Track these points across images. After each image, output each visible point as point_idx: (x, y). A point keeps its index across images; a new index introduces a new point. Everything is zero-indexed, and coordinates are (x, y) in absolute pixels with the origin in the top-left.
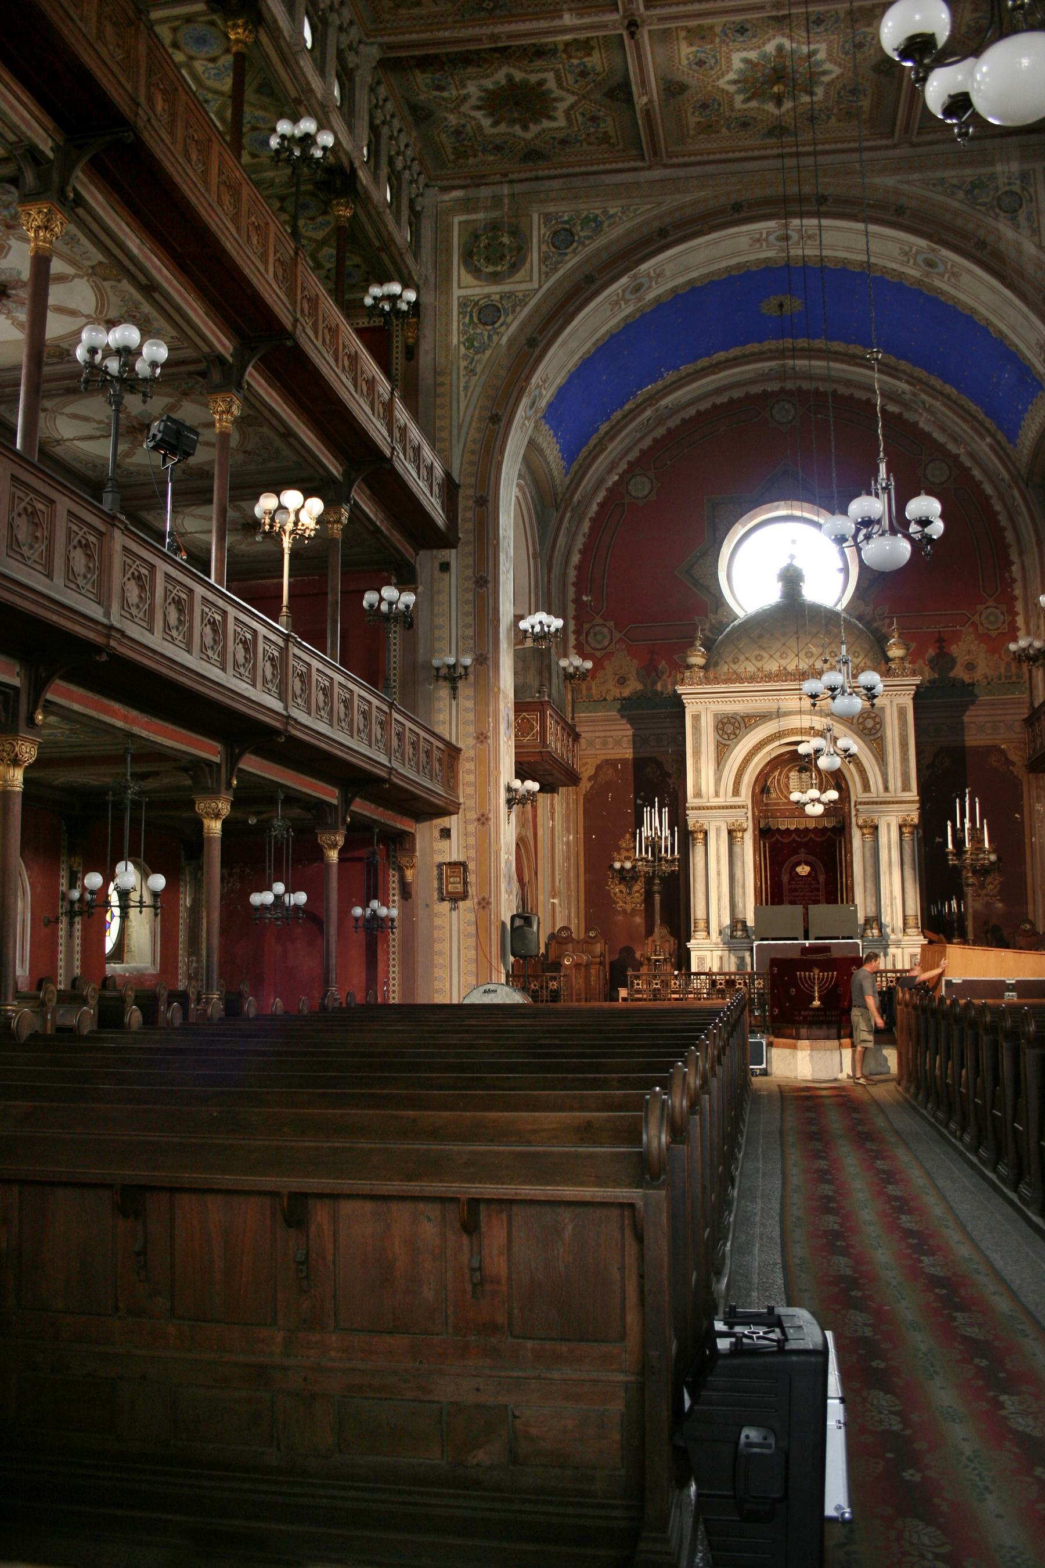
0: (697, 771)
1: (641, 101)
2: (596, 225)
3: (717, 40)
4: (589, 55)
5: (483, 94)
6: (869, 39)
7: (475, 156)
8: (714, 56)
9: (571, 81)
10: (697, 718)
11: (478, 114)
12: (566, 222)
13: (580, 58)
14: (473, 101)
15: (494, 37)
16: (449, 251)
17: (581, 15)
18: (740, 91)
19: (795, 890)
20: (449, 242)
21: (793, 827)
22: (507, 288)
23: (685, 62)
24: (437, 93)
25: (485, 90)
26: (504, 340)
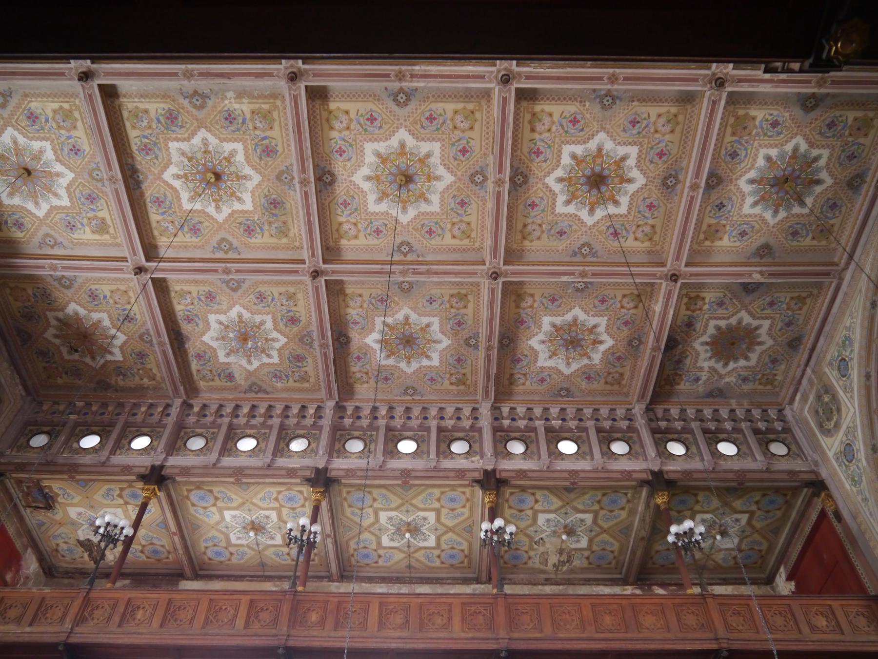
1: (757, 278)
2: (847, 341)
3: (724, 222)
4: (703, 299)
5: (713, 360)
6: (770, 118)
7: (775, 375)
8: (739, 225)
9: (725, 312)
11: (732, 365)
12: (838, 356)
13: (705, 304)
14: (719, 366)
15: (653, 349)
16: (815, 435)
17: (657, 301)
18: (789, 208)
20: (811, 429)
22: (844, 427)
23: (738, 244)
24: (700, 382)
25: (710, 358)
26: (864, 461)
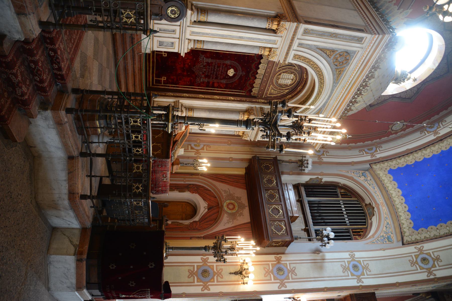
0: (322, 35)
10: (360, 40)
19: (219, 67)
21: (259, 71)
